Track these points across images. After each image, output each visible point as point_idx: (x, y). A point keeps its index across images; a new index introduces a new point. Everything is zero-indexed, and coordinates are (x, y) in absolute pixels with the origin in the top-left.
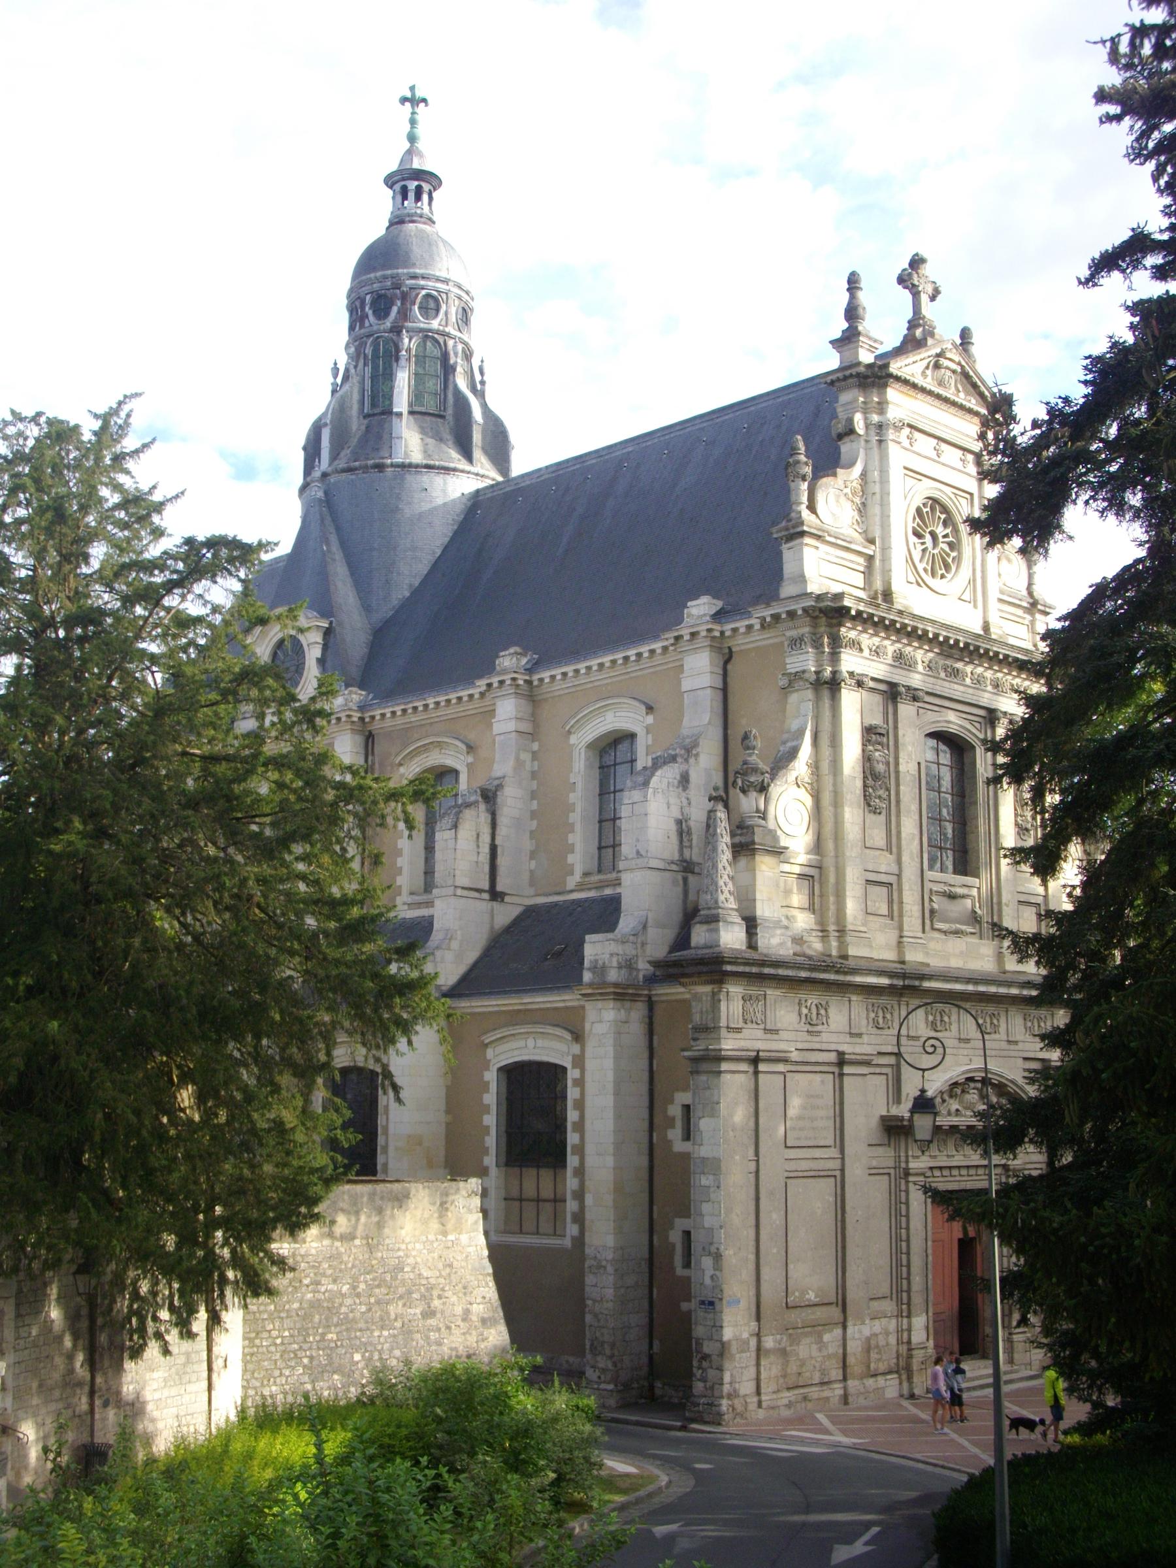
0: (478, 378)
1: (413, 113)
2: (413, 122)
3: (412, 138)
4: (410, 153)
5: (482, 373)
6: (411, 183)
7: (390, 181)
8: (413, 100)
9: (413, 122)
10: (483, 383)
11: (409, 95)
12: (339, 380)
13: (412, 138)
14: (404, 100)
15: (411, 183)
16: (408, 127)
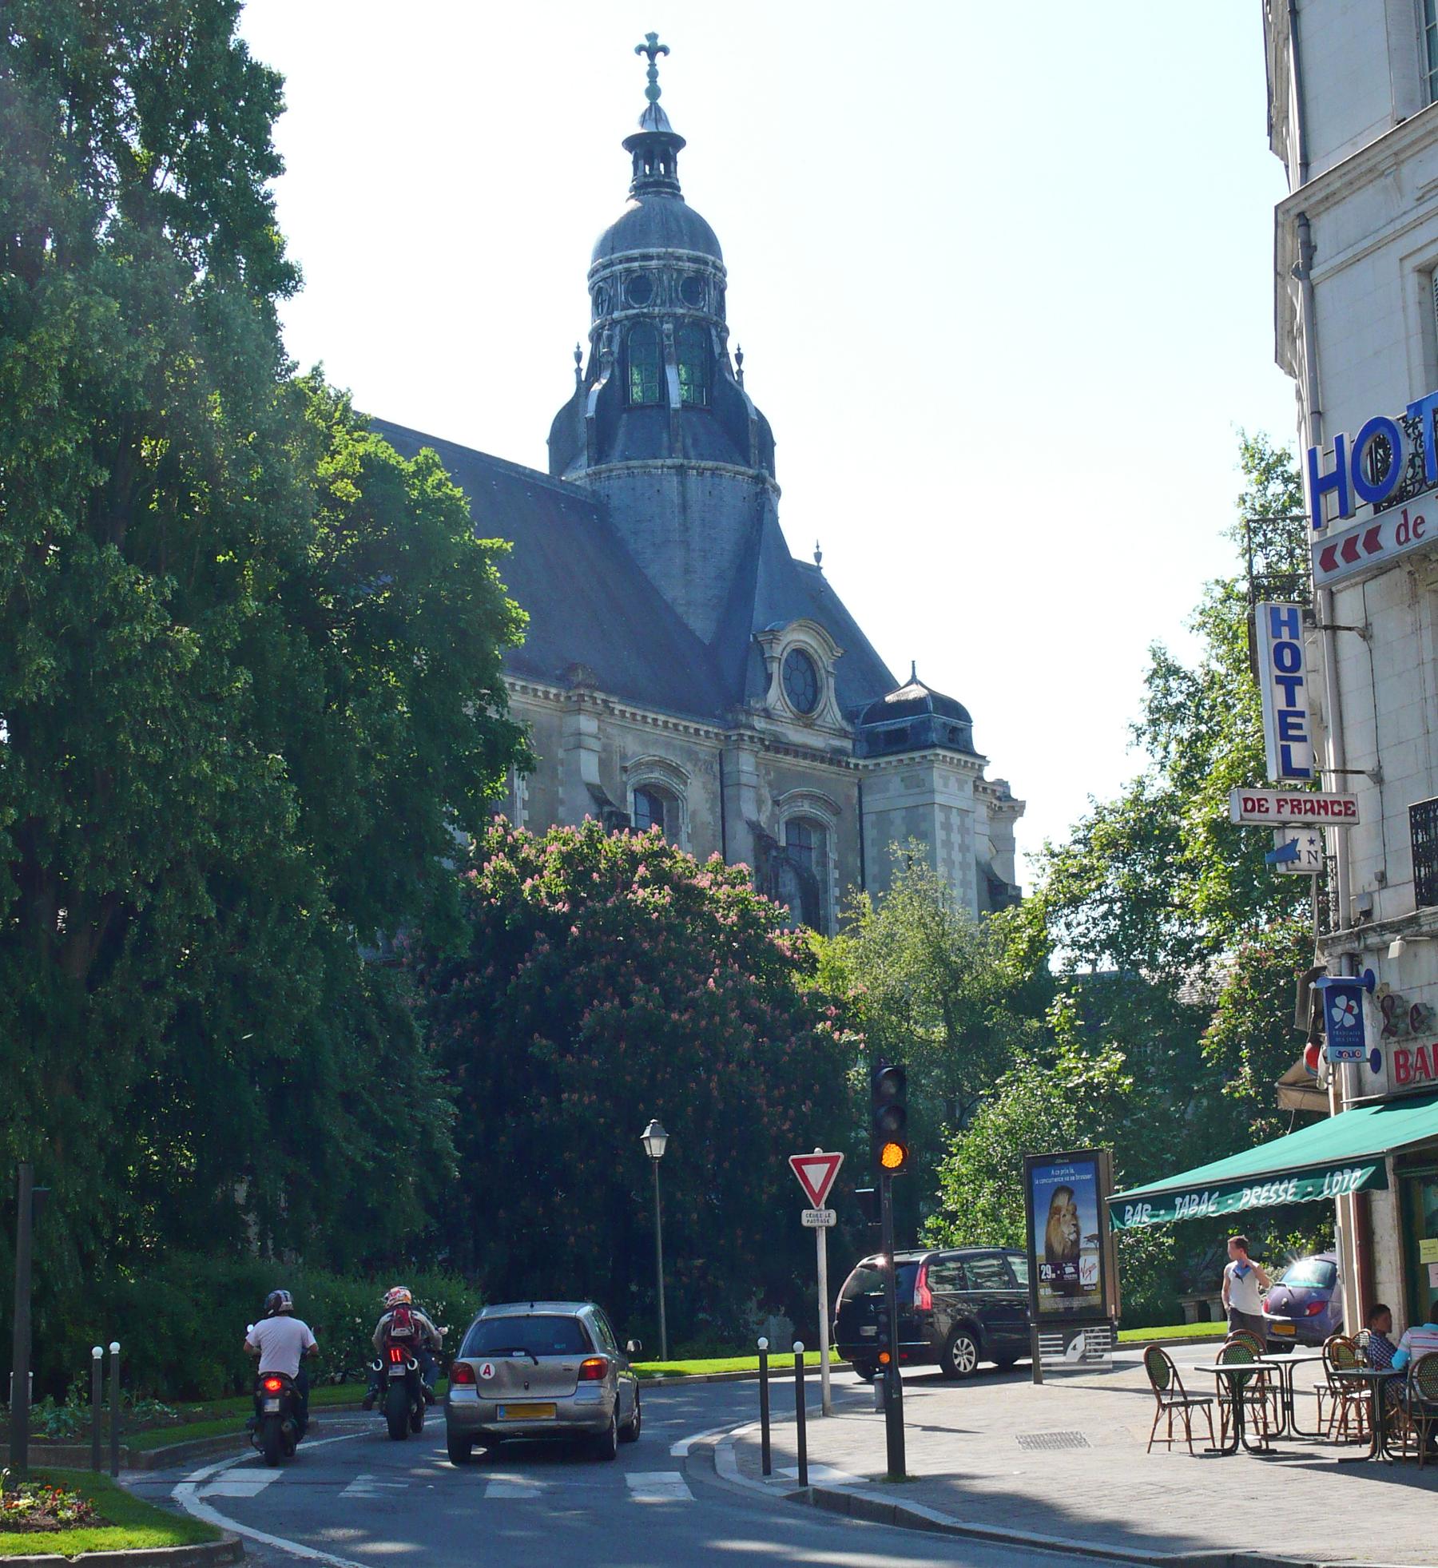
0: (735, 367)
1: (652, 65)
2: (653, 74)
3: (653, 92)
4: (654, 113)
5: (739, 358)
6: (655, 149)
7: (631, 143)
8: (652, 49)
9: (653, 74)
10: (740, 372)
11: (647, 44)
12: (584, 364)
13: (653, 92)
14: (640, 49)
15: (655, 149)
16: (646, 83)
